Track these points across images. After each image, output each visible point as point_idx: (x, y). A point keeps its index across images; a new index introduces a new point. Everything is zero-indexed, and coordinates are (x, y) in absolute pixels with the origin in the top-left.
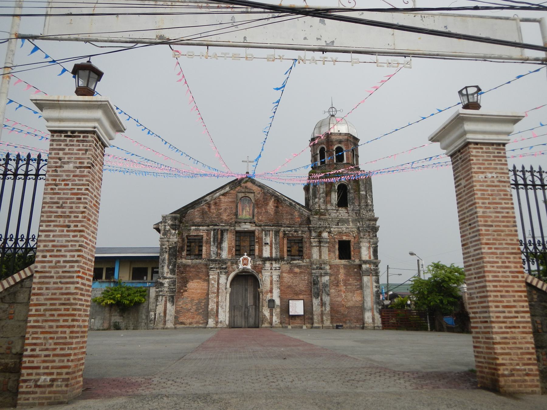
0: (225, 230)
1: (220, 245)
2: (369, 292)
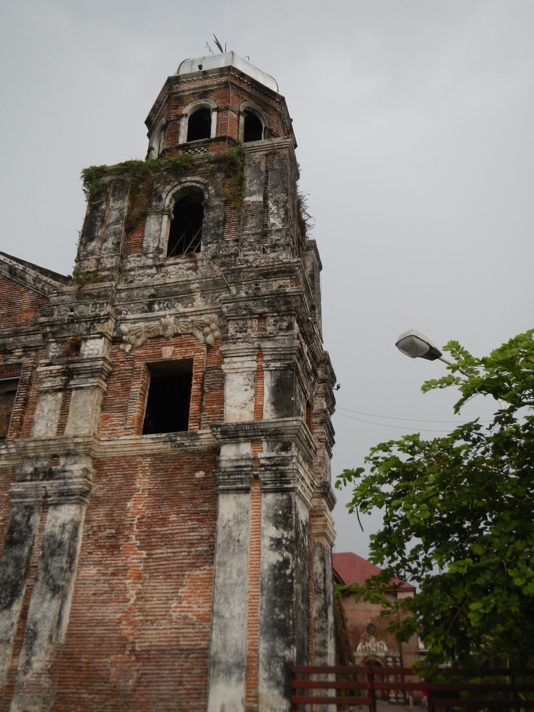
2: (240, 572)
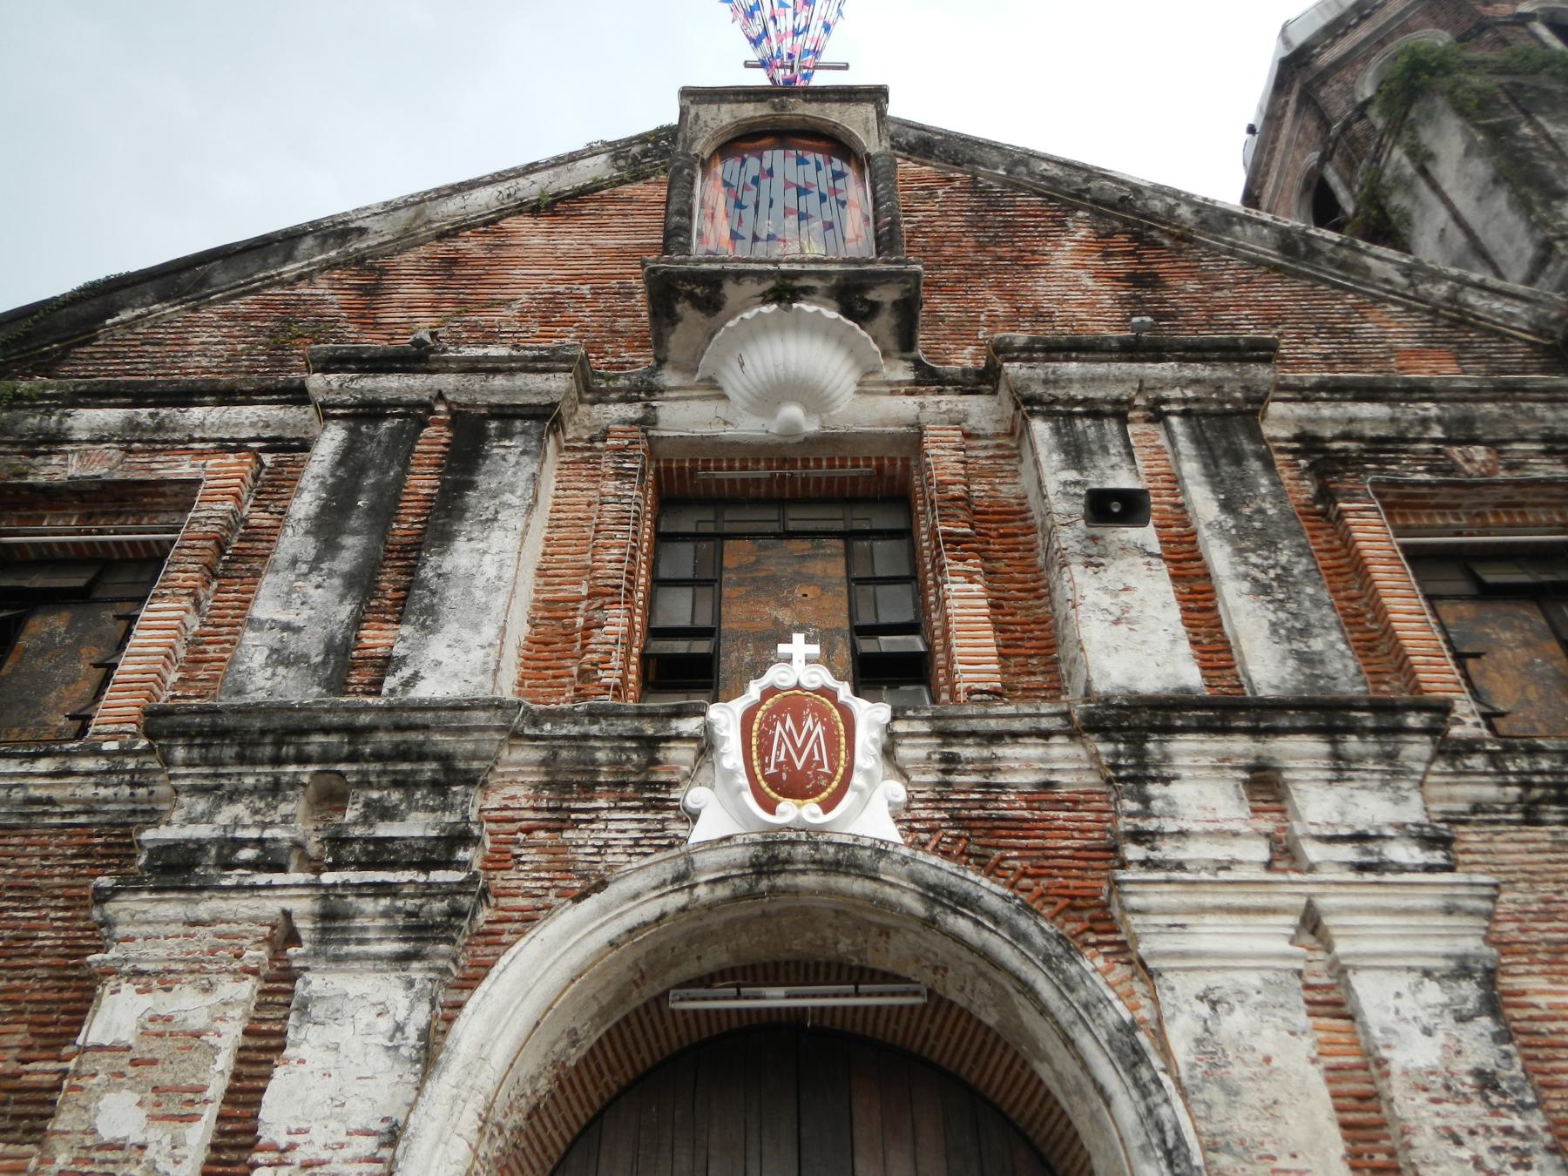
0: (507, 414)
1: (412, 570)
